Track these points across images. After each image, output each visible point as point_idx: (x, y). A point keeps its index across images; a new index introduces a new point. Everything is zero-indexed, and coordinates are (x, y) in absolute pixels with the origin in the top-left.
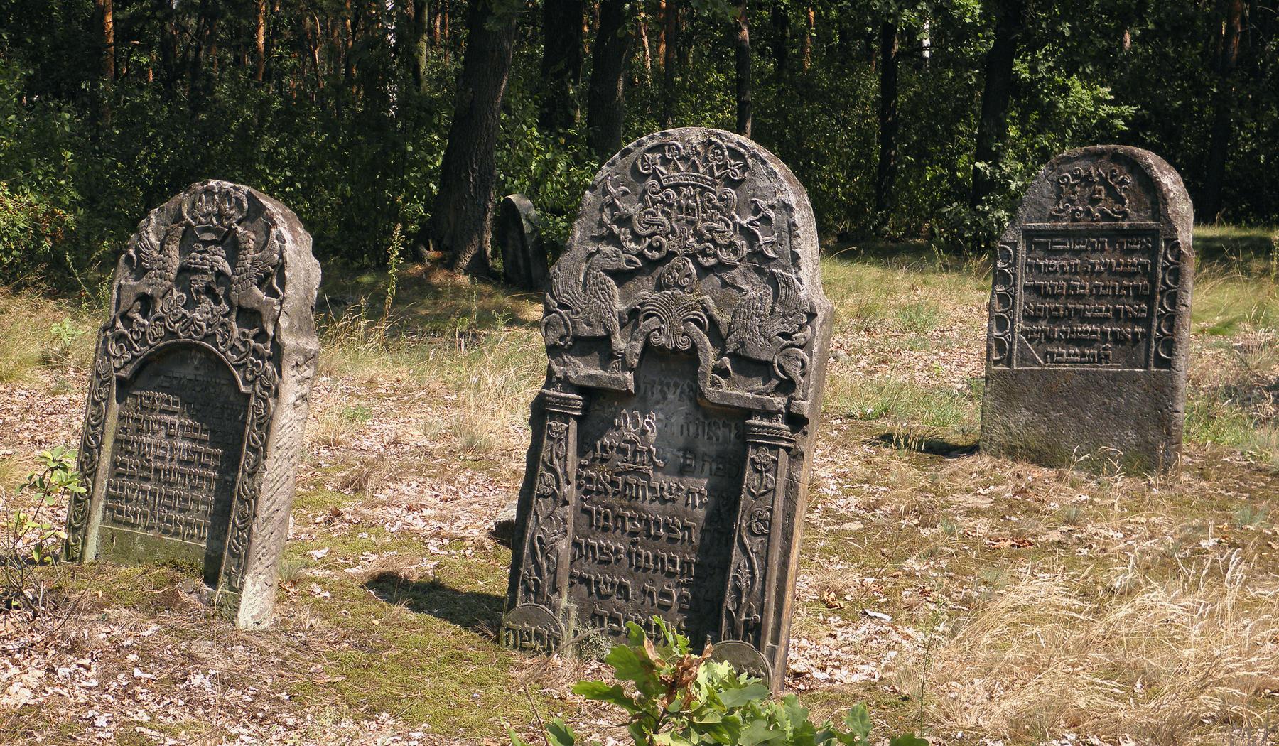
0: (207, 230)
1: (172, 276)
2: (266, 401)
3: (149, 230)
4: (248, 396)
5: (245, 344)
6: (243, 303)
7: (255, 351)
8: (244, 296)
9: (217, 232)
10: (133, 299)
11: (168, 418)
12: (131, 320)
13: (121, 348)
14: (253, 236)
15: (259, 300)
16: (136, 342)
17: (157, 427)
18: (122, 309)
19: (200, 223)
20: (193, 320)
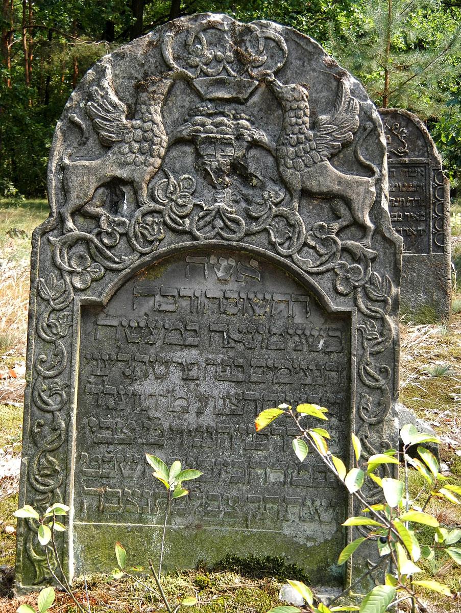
0: (221, 83)
1: (163, 151)
2: (382, 319)
3: (105, 84)
4: (345, 318)
5: (325, 242)
6: (313, 185)
7: (345, 250)
8: (310, 176)
9: (240, 86)
10: (93, 186)
11: (181, 356)
12: (96, 218)
13: (81, 257)
14: (306, 92)
15: (340, 181)
16: (110, 248)
17: (161, 370)
18: (74, 202)
19: (206, 75)
20: (219, 213)
